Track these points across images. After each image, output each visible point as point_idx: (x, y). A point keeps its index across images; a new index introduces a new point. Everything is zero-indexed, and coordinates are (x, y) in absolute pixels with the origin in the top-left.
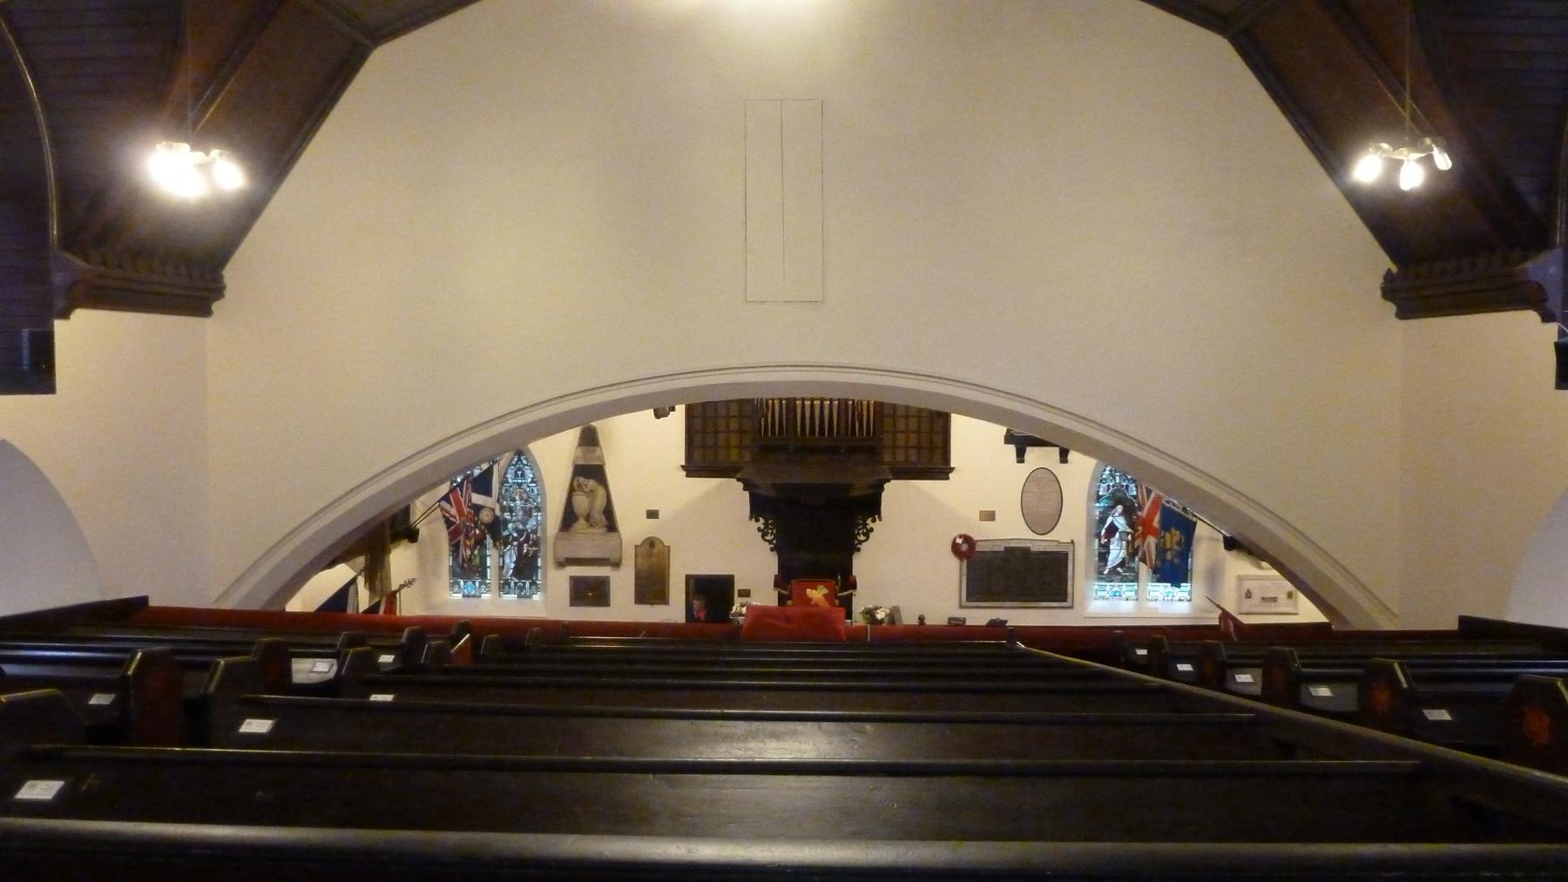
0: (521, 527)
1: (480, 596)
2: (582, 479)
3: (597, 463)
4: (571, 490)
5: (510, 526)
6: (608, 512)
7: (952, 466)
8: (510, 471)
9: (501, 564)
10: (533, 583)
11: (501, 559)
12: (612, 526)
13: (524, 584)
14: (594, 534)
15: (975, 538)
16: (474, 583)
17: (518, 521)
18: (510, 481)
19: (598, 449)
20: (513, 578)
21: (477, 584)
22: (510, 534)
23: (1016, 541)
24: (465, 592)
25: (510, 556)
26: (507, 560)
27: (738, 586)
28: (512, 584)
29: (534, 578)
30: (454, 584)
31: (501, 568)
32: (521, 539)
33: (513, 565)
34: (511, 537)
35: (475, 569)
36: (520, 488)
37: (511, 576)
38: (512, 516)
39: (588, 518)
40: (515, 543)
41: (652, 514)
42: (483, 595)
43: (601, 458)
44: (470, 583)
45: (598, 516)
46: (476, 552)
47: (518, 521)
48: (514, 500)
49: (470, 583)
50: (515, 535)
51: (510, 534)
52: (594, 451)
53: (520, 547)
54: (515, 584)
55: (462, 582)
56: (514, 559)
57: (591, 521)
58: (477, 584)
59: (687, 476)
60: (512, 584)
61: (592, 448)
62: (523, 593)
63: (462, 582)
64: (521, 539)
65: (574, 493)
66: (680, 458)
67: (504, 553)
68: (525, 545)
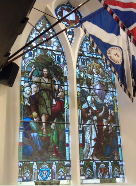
0: (99, 101)
1: (58, 184)
5: (89, 98)
8: (85, 45)
9: (81, 142)
10: (116, 164)
11: (81, 136)
13: (107, 165)
16: (50, 166)
17: (96, 94)
18: (86, 54)
20: (95, 159)
21: (54, 167)
22: (90, 108)
24: (40, 178)
25: (91, 132)
26: (88, 138)
28: (94, 166)
29: (116, 159)
30: (25, 167)
31: (82, 146)
32: (101, 114)
33: (93, 143)
34: (90, 111)
35: (51, 146)
36: (95, 62)
37: (92, 156)
38: (90, 89)
40: (95, 118)
42: (62, 182)
44: (45, 166)
46: (53, 126)
47: (96, 94)
48: (92, 73)
49: (45, 166)
50: (94, 108)
51: (90, 108)
53: (100, 121)
54: (98, 165)
55: (35, 165)
56: (95, 136)
58: (54, 167)
60: (94, 166)
62: (106, 177)
63: (35, 165)
64: (101, 114)
67: (83, 128)
68: (105, 120)
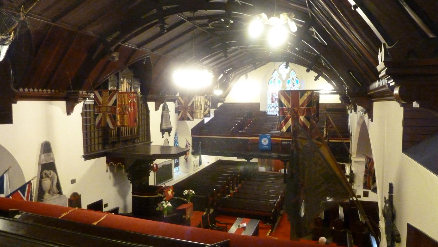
2: (46, 171)
3: (51, 161)
4: (41, 177)
6: (58, 186)
7: (151, 141)
12: (60, 193)
14: (54, 199)
15: (157, 164)
19: (52, 154)
23: (164, 163)
27: (104, 203)
39: (49, 192)
41: (73, 181)
43: (53, 159)
45: (55, 188)
52: (50, 155)
57: (51, 192)
59: (85, 160)
61: (49, 154)
65: (43, 180)
66: (81, 151)
